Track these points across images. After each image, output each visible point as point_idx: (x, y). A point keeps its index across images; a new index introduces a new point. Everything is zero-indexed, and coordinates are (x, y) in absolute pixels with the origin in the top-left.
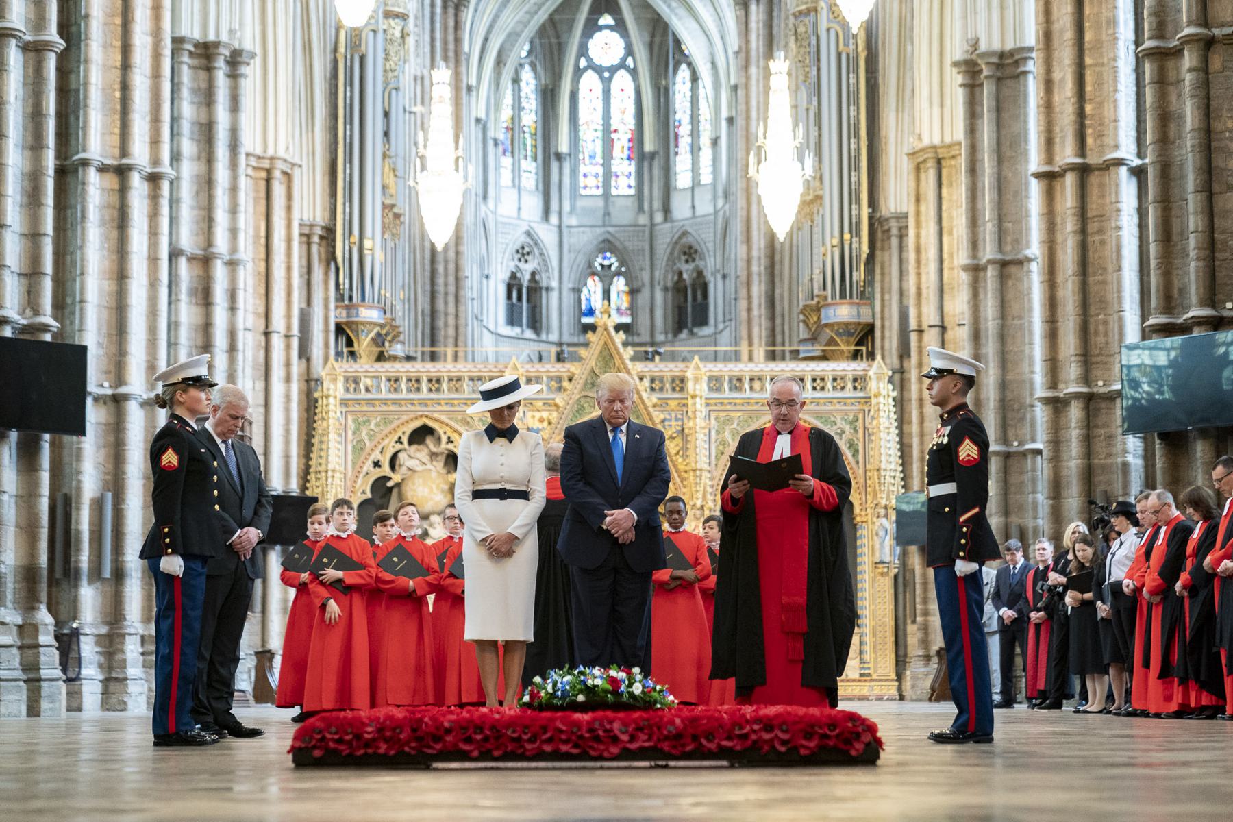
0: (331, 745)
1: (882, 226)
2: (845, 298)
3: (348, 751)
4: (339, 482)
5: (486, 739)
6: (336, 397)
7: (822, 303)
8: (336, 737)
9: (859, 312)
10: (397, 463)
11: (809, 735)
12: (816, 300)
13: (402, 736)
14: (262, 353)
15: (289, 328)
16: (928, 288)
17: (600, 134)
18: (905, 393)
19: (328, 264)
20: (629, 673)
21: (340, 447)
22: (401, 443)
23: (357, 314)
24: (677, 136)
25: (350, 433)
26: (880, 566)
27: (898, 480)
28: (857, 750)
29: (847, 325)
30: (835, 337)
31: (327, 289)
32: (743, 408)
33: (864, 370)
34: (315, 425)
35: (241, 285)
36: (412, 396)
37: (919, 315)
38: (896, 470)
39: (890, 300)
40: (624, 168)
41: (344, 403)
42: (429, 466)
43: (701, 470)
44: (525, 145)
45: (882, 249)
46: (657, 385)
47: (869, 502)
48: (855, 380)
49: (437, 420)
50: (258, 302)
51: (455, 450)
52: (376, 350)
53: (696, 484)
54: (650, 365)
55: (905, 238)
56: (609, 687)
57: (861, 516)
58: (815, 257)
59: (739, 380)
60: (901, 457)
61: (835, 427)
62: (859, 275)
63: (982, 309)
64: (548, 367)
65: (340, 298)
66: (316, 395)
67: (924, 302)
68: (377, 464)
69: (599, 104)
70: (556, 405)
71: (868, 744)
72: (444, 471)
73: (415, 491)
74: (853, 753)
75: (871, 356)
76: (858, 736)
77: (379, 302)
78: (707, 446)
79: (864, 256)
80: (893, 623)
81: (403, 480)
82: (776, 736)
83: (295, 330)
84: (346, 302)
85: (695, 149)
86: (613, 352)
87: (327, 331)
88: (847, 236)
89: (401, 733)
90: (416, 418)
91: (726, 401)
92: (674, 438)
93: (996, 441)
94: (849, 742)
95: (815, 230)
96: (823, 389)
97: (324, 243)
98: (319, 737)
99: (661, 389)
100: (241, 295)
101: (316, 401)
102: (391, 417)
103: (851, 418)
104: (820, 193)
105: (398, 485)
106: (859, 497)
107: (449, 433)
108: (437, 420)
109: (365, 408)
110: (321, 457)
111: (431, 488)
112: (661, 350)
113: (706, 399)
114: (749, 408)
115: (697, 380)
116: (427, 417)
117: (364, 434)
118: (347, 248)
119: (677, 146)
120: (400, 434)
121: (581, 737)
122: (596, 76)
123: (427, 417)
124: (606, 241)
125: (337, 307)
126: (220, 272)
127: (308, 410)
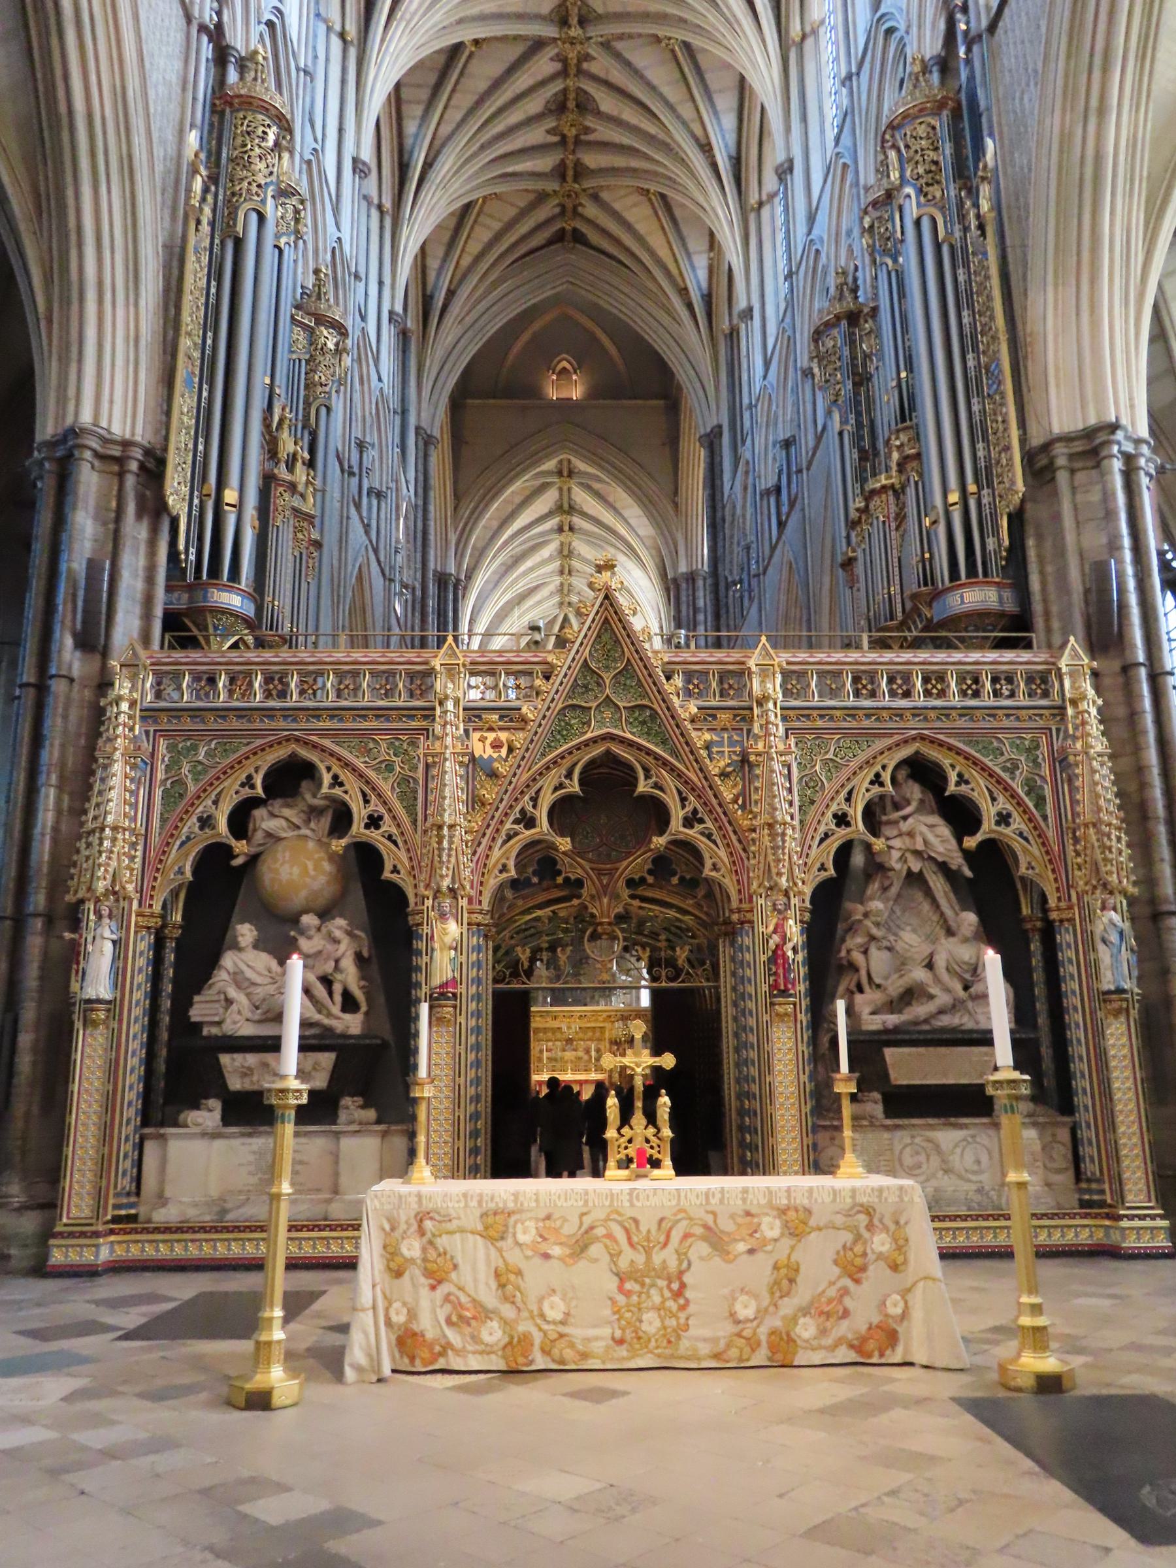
2: (976, 576)
36: (271, 703)
41: (149, 715)
57: (1058, 909)
61: (1001, 759)
70: (524, 720)
87: (147, 616)
88: (972, 488)
107: (336, 769)
116: (297, 740)
117: (185, 770)
118: (196, 501)
123: (297, 740)
125: (169, 589)
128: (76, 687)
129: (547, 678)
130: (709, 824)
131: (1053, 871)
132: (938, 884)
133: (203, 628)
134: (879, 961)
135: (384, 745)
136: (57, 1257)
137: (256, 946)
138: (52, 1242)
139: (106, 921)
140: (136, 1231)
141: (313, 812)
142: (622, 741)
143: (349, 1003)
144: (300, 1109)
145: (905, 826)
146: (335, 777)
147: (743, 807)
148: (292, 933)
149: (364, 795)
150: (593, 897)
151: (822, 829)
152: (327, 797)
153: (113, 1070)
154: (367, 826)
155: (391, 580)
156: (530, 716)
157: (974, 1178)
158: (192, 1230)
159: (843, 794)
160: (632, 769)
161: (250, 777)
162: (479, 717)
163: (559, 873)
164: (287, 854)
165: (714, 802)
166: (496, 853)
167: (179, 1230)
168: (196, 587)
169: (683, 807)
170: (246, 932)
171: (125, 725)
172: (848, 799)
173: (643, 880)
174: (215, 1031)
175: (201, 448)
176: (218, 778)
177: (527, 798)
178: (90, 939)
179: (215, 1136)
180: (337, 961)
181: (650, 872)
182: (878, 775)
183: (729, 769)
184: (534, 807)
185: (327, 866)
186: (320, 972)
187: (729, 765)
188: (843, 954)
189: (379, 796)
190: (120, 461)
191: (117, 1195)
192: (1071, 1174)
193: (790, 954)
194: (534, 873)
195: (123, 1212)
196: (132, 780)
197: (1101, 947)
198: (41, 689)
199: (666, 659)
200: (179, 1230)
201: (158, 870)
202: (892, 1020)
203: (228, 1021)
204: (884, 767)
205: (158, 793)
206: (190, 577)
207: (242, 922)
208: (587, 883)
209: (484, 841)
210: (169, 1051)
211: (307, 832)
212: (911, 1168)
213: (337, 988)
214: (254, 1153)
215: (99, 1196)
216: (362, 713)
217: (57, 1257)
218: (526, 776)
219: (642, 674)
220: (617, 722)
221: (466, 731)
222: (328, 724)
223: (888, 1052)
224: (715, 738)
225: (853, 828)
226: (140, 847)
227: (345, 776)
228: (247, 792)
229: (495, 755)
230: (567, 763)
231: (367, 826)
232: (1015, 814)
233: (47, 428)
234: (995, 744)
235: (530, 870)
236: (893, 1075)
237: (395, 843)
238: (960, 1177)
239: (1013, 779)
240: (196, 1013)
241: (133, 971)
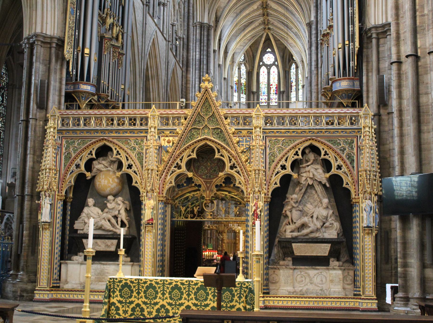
1: (367, 35)
17: (266, 86)
18: (381, 127)
24: (291, 86)
25: (64, 149)
29: (347, 91)
31: (61, 73)
32: (286, 135)
38: (376, 172)
39: (372, 76)
40: (274, 97)
41: (60, 131)
43: (259, 170)
44: (242, 89)
47: (360, 190)
62: (353, 64)
67: (402, 43)
69: (266, 77)
70: (178, 133)
73: (100, 182)
79: (356, 49)
85: (297, 90)
86: (211, 103)
87: (60, 96)
88: (347, 42)
91: (275, 131)
92: (245, 152)
104: (331, 24)
106: (354, 187)
114: (289, 134)
116: (106, 140)
117: (71, 149)
118: (75, 53)
119: (291, 89)
122: (265, 68)
123: (106, 140)
125: (67, 84)
128: (38, 121)
129: (186, 119)
130: (238, 169)
131: (354, 186)
132: (319, 188)
133: (79, 97)
134: (295, 214)
135: (133, 142)
136: (37, 297)
137: (94, 205)
138: (35, 292)
139: (48, 198)
140: (59, 290)
141: (113, 162)
142: (210, 140)
143: (123, 225)
144: (93, 256)
145: (307, 169)
146: (118, 152)
147: (249, 163)
148: (105, 202)
149: (127, 158)
150: (204, 191)
151: (276, 171)
152: (115, 158)
153: (52, 243)
154: (128, 168)
155: (168, 41)
156: (180, 132)
157: (320, 286)
158: (75, 291)
159: (284, 159)
160: (214, 150)
161: (91, 152)
162: (163, 132)
163: (193, 182)
164: (104, 176)
165: (240, 161)
166: (169, 177)
167: (72, 291)
168: (76, 84)
169: (230, 162)
170: (91, 201)
171: (52, 136)
172: (286, 160)
173: (221, 185)
174: (81, 232)
175: (77, 34)
176: (81, 152)
177: (179, 159)
178: (43, 204)
179: (82, 264)
180: (119, 211)
181: (224, 182)
182: (297, 152)
183: (245, 150)
184: (181, 162)
185: (116, 180)
186: (113, 215)
187: (245, 149)
188: (284, 212)
189: (131, 158)
190: (50, 43)
191: (53, 280)
192: (353, 285)
193: (259, 213)
194: (185, 182)
195: (55, 285)
196: (55, 153)
197: (364, 212)
198: (27, 121)
199: (225, 113)
200: (72, 291)
201: (63, 181)
202: (295, 234)
203: (85, 229)
204: (299, 149)
205: (63, 157)
206: (74, 78)
207: (90, 198)
208: (202, 186)
209: (164, 174)
210: (69, 237)
211: (110, 169)
212: (299, 282)
213: (119, 220)
214: (94, 269)
215: (49, 280)
216: (126, 131)
217: (37, 297)
218: (178, 152)
219: (218, 117)
220: (208, 134)
221: (159, 137)
222: (115, 135)
223: (294, 245)
224: (241, 139)
225: (287, 170)
226: (58, 175)
227: (121, 151)
228: (90, 156)
229: (168, 145)
230: (192, 147)
231: (128, 168)
232: (344, 166)
233: (26, 33)
234: (338, 141)
235: (184, 181)
236: (295, 252)
237: (136, 173)
238: (316, 285)
239: (343, 154)
240: (76, 226)
241: (56, 213)
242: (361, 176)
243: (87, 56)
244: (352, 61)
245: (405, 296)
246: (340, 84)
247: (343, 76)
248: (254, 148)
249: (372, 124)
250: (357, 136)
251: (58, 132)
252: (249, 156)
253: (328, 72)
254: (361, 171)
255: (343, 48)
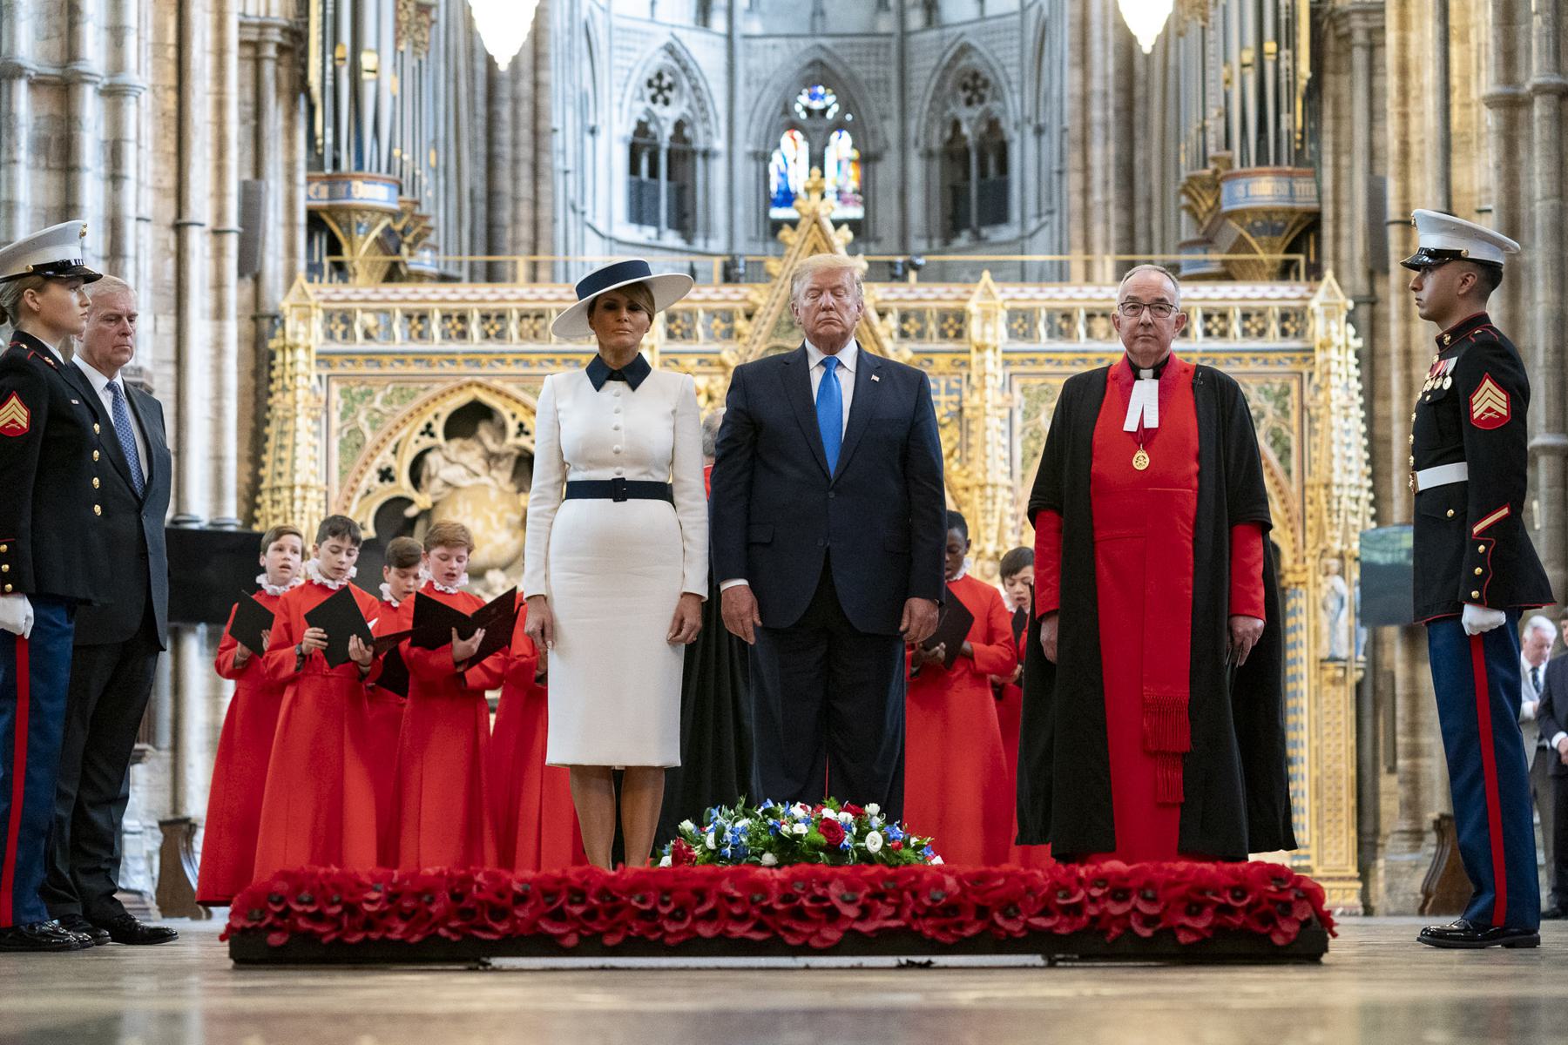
0: (302, 923)
1: (1336, 28)
2: (1267, 163)
3: (332, 936)
4: (315, 508)
5: (591, 914)
6: (308, 349)
7: (1223, 172)
8: (311, 909)
9: (1291, 189)
10: (425, 472)
11: (1194, 909)
12: (1212, 166)
13: (433, 909)
14: (170, 264)
15: (220, 215)
16: (1422, 142)
18: (1377, 341)
19: (294, 101)
20: (859, 814)
21: (316, 441)
22: (432, 435)
23: (349, 192)
25: (335, 416)
26: (1330, 665)
27: (1364, 504)
28: (1286, 934)
29: (1269, 213)
30: (1248, 236)
31: (291, 146)
33: (1302, 298)
34: (270, 401)
35: (131, 133)
37: (1405, 194)
38: (1360, 487)
39: (1351, 167)
41: (324, 358)
42: (484, 479)
43: (994, 486)
45: (1337, 72)
46: (912, 326)
47: (1310, 545)
48: (1284, 317)
49: (499, 392)
50: (162, 168)
51: (533, 448)
52: (384, 260)
53: (985, 512)
54: (900, 290)
55: (1378, 51)
56: (822, 839)
57: (1294, 571)
58: (1210, 86)
59: (1067, 316)
60: (1370, 462)
62: (1294, 120)
63: (1523, 178)
64: (708, 292)
65: (315, 162)
66: (272, 344)
67: (1414, 169)
68: (386, 475)
70: (723, 364)
71: (1306, 924)
72: (512, 488)
74: (1279, 940)
75: (1315, 272)
76: (1288, 907)
77: (389, 170)
78: (1006, 441)
79: (1302, 83)
80: (1353, 772)
81: (435, 504)
82: (1135, 909)
83: (233, 221)
84: (329, 171)
87: (291, 224)
88: (1270, 46)
89: (430, 903)
90: (461, 388)
91: (1042, 357)
93: (1547, 426)
94: (1269, 919)
95: (1211, 35)
96: (1223, 334)
97: (286, 59)
98: (278, 909)
99: (920, 335)
100: (130, 152)
101: (272, 356)
102: (413, 387)
103: (1277, 388)
105: (426, 514)
107: (521, 417)
108: (499, 392)
109: (364, 370)
110: (281, 460)
111: (488, 520)
112: (921, 261)
113: (1005, 352)
115: (987, 316)
116: (479, 386)
117: (362, 419)
118: (329, 68)
120: (429, 417)
121: (769, 910)
123: (479, 386)
124: (816, 63)
125: (310, 180)
126: (91, 108)
127: (256, 373)
197: (1321, 613)
199: (879, 297)
242: (1311, 503)
243: (370, 80)
244: (1288, 111)
245: (1415, 827)
246: (1247, 188)
247: (1259, 163)
248: (976, 413)
249: (1346, 335)
250: (1301, 374)
251: (318, 361)
252: (957, 439)
253: (1204, 118)
254: (1312, 487)
255: (1256, 65)
